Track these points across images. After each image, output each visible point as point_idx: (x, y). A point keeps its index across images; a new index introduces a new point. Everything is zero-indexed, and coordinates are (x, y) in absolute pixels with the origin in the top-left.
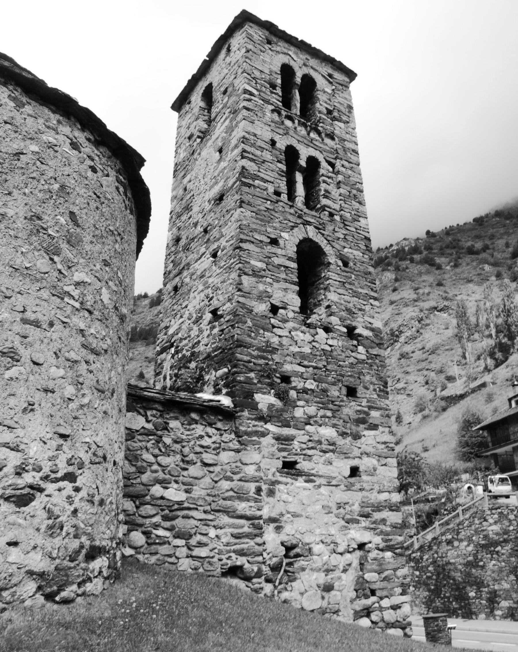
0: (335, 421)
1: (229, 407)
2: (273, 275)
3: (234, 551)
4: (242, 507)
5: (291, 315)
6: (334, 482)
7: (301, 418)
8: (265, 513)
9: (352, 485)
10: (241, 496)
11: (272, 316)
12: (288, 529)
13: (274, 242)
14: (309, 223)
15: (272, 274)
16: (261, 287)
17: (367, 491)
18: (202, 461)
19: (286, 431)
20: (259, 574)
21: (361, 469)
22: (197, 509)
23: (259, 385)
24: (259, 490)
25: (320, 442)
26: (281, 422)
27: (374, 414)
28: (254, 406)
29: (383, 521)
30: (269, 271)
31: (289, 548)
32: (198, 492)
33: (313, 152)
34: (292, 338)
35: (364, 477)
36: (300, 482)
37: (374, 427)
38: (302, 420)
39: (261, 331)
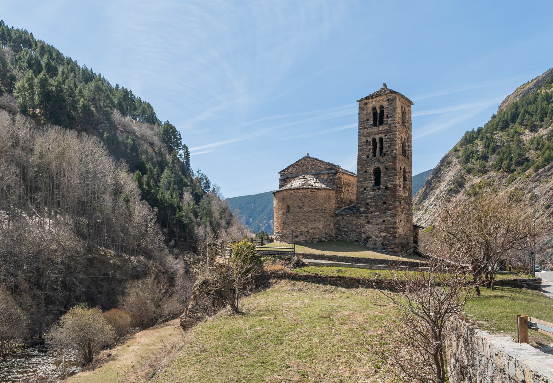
4: (358, 230)
5: (369, 189)
8: (362, 231)
10: (357, 228)
12: (367, 234)
13: (366, 172)
14: (376, 162)
16: (362, 185)
19: (367, 215)
20: (361, 242)
24: (361, 227)
27: (390, 207)
29: (391, 231)
31: (367, 237)
32: (349, 228)
33: (381, 135)
36: (370, 225)
37: (391, 210)
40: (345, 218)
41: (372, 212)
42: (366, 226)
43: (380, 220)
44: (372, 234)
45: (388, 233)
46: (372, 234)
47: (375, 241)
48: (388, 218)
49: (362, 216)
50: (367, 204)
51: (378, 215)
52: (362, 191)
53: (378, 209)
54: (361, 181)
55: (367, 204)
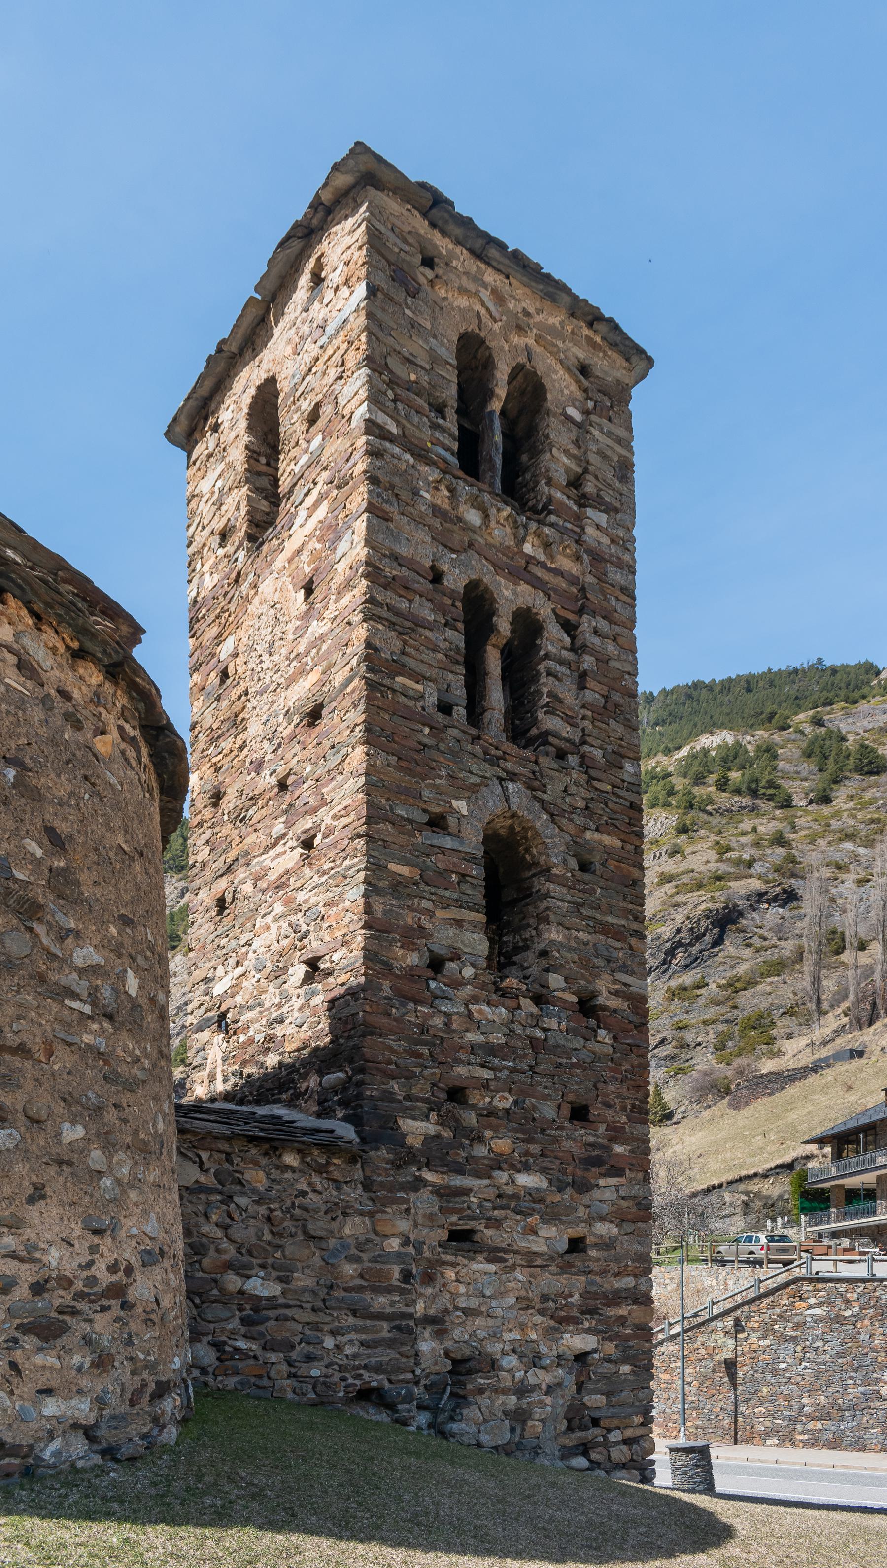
0: (546, 1162)
1: (350, 1142)
2: (435, 894)
3: (365, 1367)
6: (538, 1262)
7: (484, 1157)
9: (571, 1265)
11: (431, 974)
15: (433, 890)
16: (410, 919)
17: (597, 1274)
18: (306, 1232)
21: (588, 1242)
22: (301, 1307)
23: (408, 1104)
25: (515, 1196)
26: (447, 1165)
28: (397, 1139)
30: (427, 884)
32: (302, 1280)
34: (470, 1015)
35: (593, 1253)
38: (486, 1162)
39: (411, 1006)
40: (257, 1178)
41: (498, 1163)
42: (450, 1274)
43: (548, 1231)
44: (495, 1336)
45: (604, 1333)
46: (495, 1336)
47: (522, 1390)
48: (602, 1229)
49: (418, 1184)
50: (457, 1095)
51: (535, 1197)
52: (411, 974)
53: (535, 1148)
54: (398, 886)
55: (457, 1095)
